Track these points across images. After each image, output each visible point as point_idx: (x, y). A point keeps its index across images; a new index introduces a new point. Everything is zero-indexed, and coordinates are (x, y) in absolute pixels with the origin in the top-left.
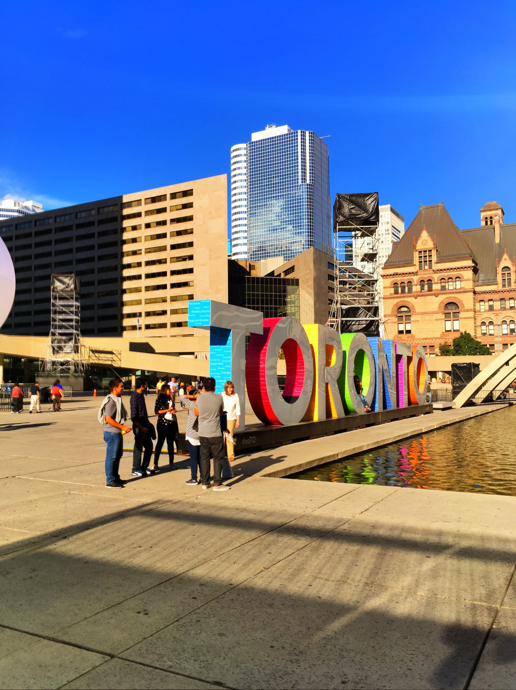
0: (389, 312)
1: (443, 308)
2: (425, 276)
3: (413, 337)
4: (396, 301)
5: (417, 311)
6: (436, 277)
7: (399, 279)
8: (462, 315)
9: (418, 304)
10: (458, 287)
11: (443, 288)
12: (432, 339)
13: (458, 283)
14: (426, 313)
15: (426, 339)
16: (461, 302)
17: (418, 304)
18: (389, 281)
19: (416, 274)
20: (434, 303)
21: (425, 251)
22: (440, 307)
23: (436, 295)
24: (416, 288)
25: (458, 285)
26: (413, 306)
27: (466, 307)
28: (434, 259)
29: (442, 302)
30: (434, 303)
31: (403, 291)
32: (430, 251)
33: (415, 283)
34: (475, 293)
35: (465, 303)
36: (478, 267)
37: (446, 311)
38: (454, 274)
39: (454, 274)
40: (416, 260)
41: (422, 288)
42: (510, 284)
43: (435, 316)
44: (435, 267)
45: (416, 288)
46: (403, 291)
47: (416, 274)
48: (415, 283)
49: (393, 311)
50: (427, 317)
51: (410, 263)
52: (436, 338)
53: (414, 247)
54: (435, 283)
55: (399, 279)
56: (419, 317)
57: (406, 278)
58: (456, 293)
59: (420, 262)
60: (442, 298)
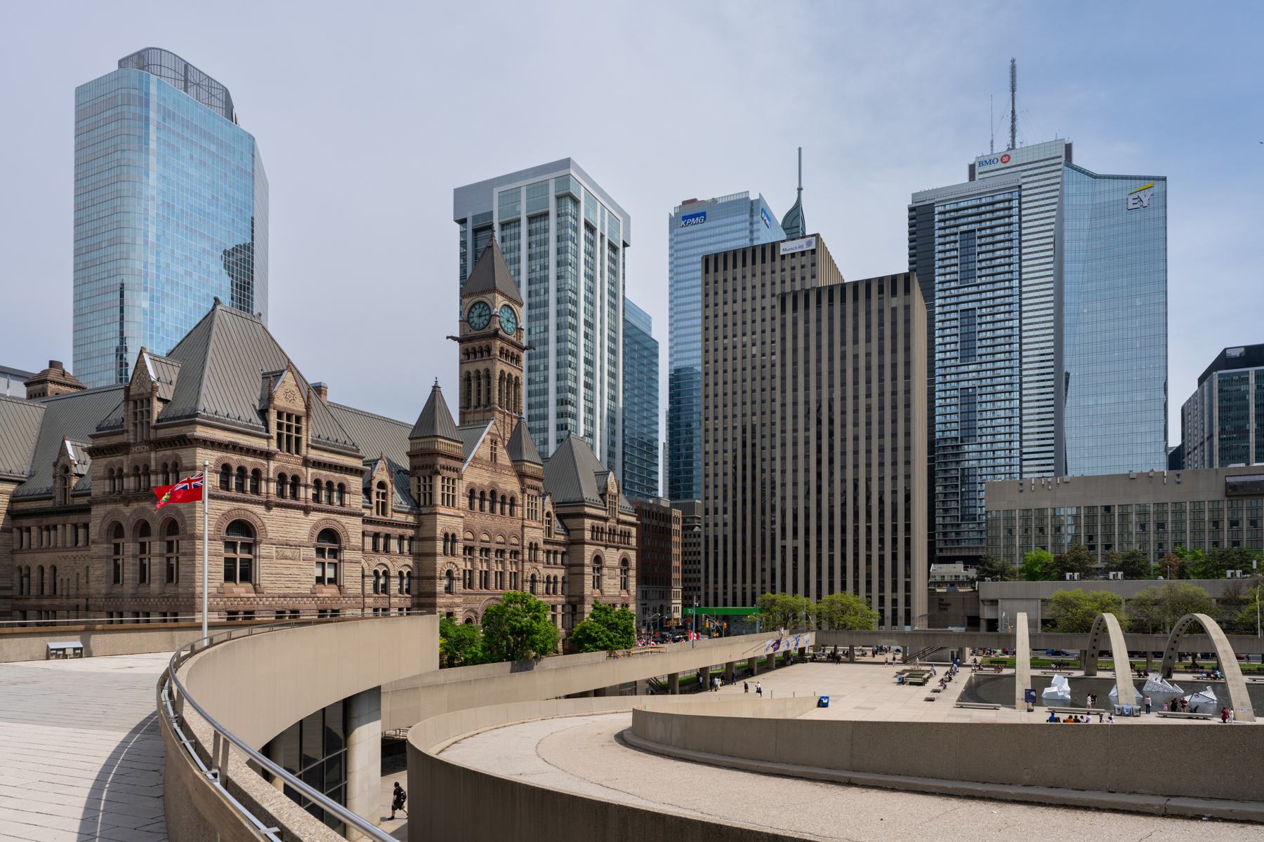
4: (227, 506)
5: (270, 535)
6: (310, 474)
7: (235, 459)
11: (316, 498)
23: (306, 510)
29: (315, 527)
31: (241, 488)
38: (336, 477)
39: (336, 477)
43: (304, 552)
46: (241, 488)
50: (288, 552)
55: (235, 459)
56: (273, 550)
60: (315, 517)
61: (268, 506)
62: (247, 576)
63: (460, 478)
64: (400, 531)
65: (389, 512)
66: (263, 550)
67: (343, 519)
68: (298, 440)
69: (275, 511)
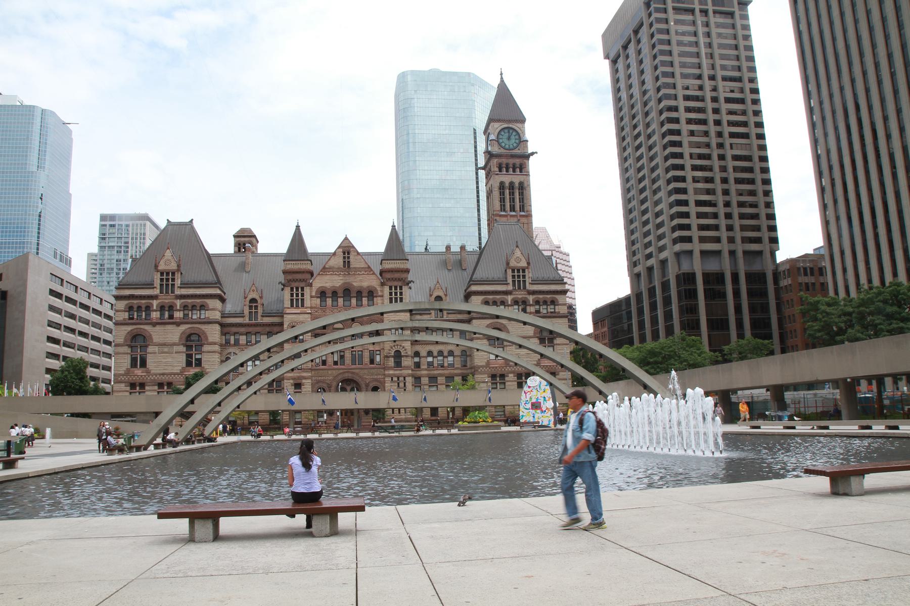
0: (121, 340)
1: (184, 339)
2: (167, 300)
3: (148, 372)
4: (130, 328)
5: (155, 341)
6: (178, 303)
8: (206, 348)
9: (158, 334)
10: (203, 317)
11: (186, 315)
12: (171, 374)
13: (203, 312)
14: (164, 345)
15: (163, 374)
16: (204, 333)
17: (158, 334)
18: (122, 305)
19: (155, 297)
20: (174, 334)
21: (168, 274)
22: (181, 338)
24: (155, 315)
25: (205, 314)
26: (151, 335)
27: (210, 339)
28: (178, 282)
29: (183, 333)
30: (174, 334)
32: (173, 274)
33: (155, 308)
34: (222, 325)
35: (208, 334)
36: (225, 297)
37: (189, 343)
40: (157, 283)
41: (162, 315)
42: (256, 318)
43: (175, 348)
44: (178, 292)
45: (155, 315)
47: (155, 297)
48: (155, 308)
49: (125, 340)
50: (166, 350)
51: (150, 285)
52: (175, 374)
53: (156, 266)
54: (177, 310)
55: (135, 302)
56: (156, 349)
57: (143, 301)
58: (200, 323)
59: (161, 285)
60: (183, 327)
61: (154, 324)
62: (144, 364)
63: (311, 285)
64: (268, 329)
65: (259, 317)
66: (150, 349)
67: (203, 327)
68: (173, 285)
69: (158, 328)
